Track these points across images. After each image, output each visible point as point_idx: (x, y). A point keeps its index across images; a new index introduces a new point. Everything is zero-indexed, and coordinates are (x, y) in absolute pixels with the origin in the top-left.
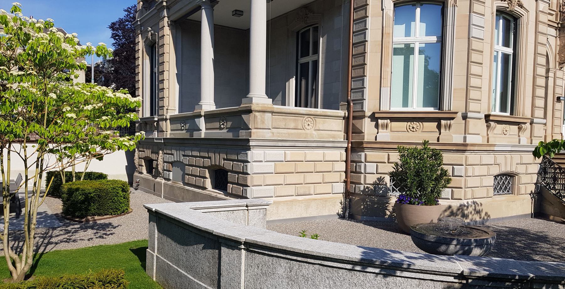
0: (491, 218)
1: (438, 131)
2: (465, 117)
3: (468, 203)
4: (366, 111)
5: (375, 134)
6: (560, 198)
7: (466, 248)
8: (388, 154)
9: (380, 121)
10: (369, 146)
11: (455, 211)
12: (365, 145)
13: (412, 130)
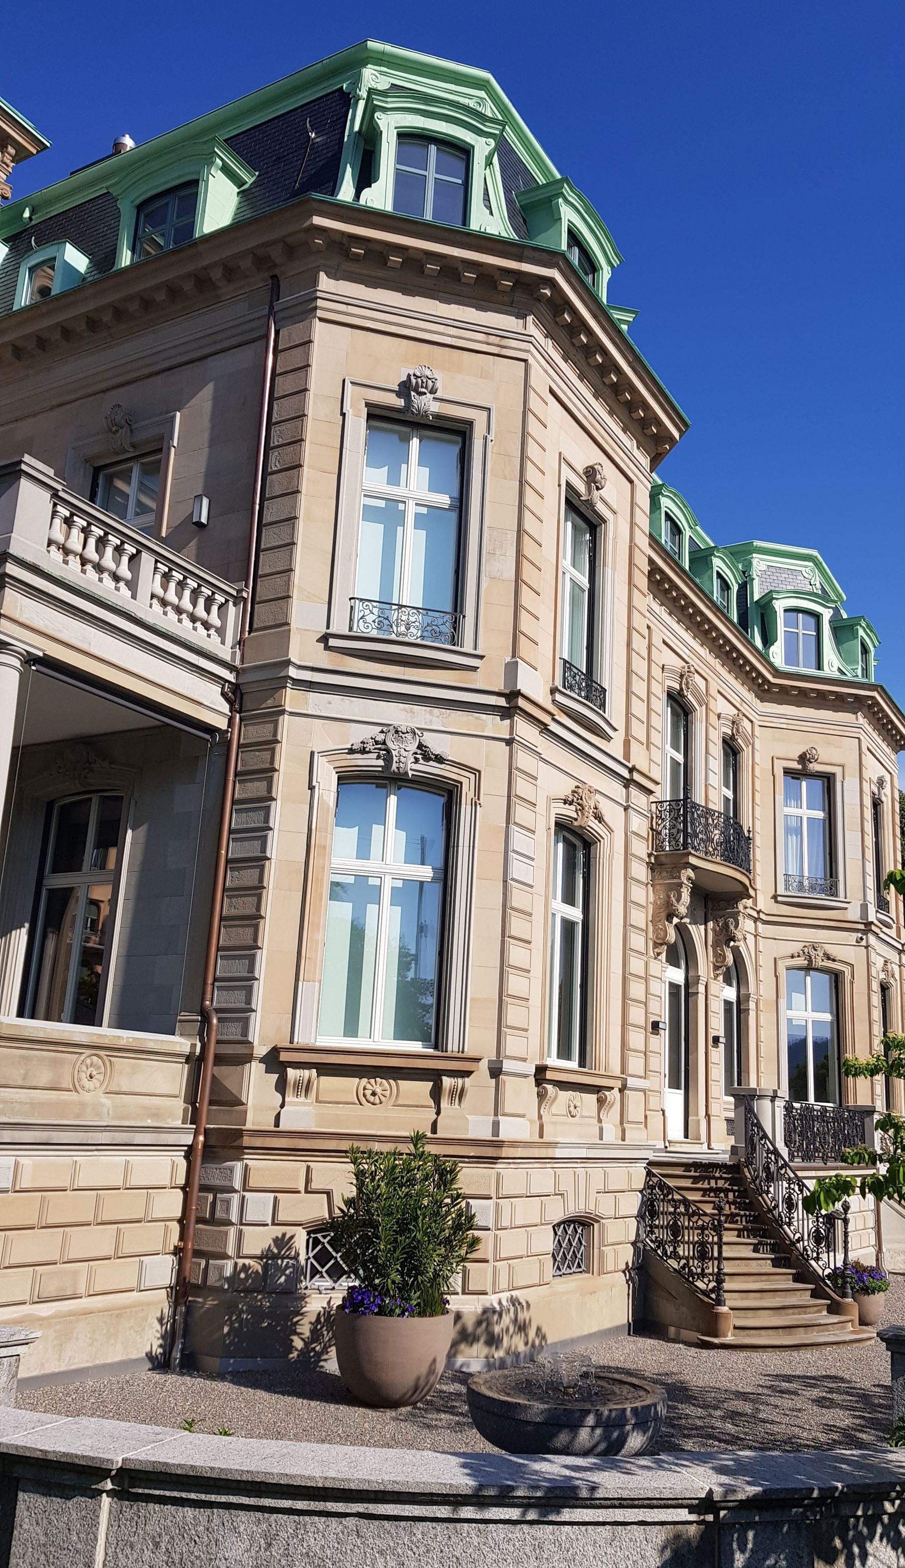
0: (549, 1342)
1: (433, 1105)
2: (496, 1072)
3: (500, 1303)
4: (256, 1043)
5: (275, 1109)
6: (691, 1279)
7: (615, 1434)
8: (308, 1168)
9: (292, 1073)
10: (258, 1142)
11: (470, 1328)
12: (247, 1141)
13: (372, 1099)
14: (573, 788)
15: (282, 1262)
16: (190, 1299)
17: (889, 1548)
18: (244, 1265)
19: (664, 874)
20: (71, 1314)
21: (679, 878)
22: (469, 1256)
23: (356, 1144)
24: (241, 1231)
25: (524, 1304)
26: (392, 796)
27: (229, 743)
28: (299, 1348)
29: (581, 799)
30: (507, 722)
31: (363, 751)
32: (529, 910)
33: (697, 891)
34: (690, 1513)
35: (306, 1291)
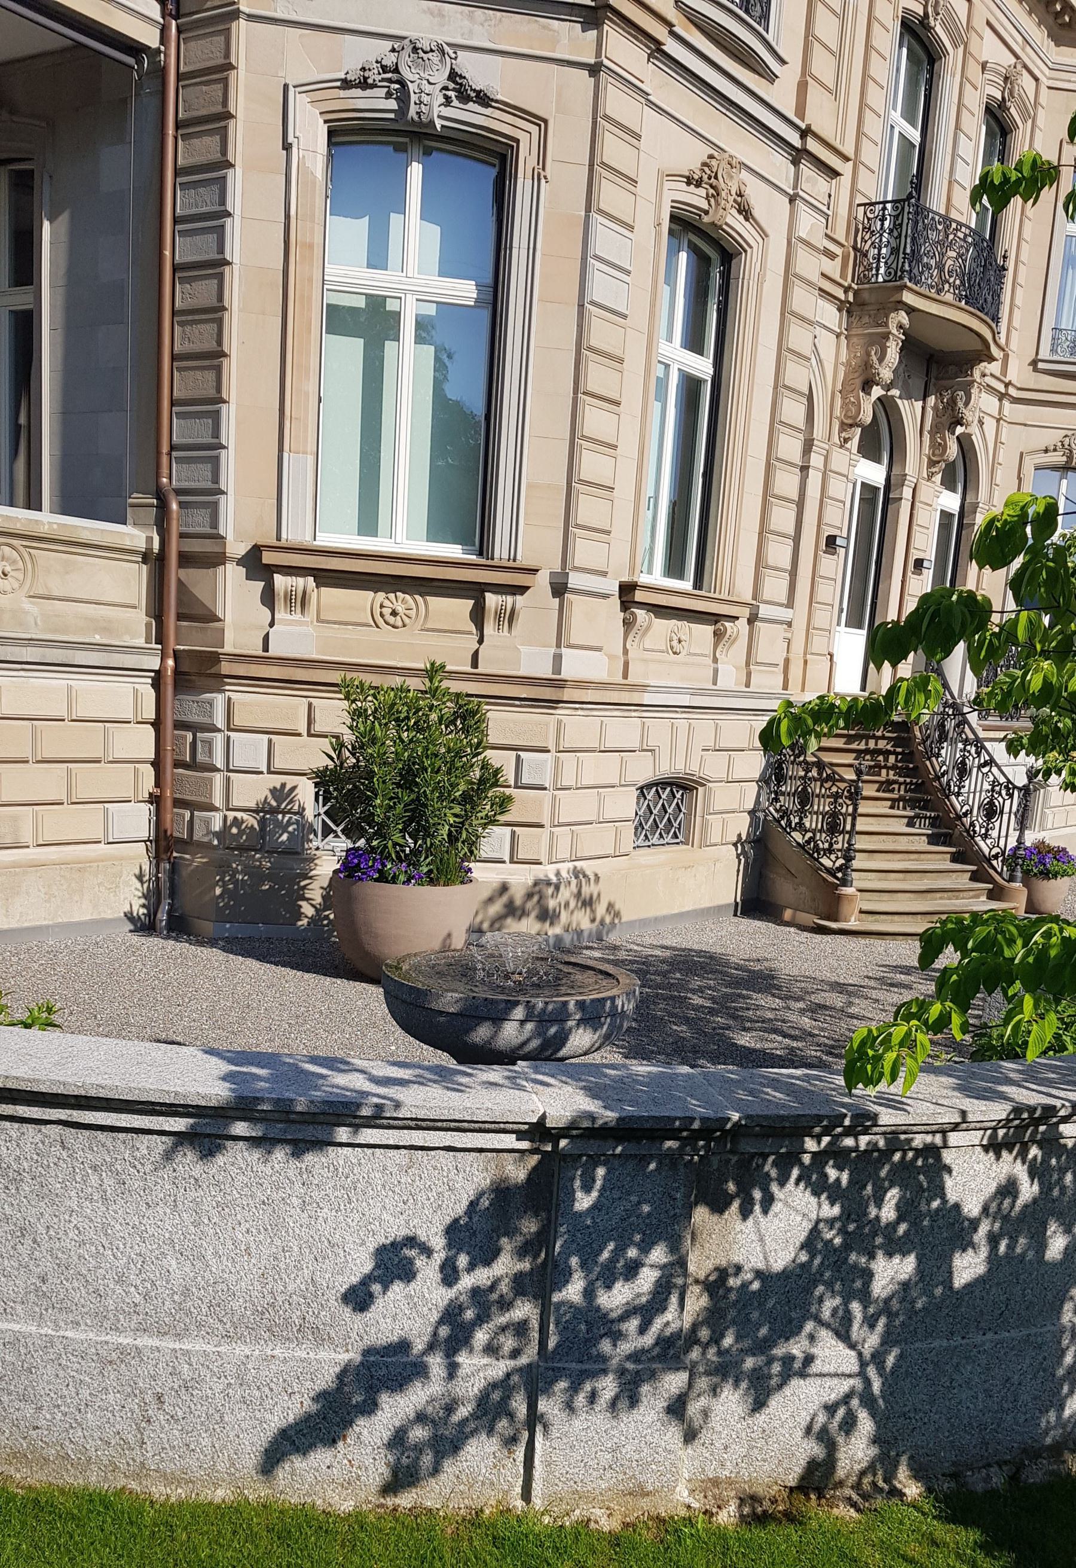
0: (623, 920)
1: (474, 631)
2: (559, 589)
3: (558, 874)
4: (230, 538)
5: (262, 627)
6: (816, 855)
7: (553, 1030)
8: (310, 705)
9: (281, 581)
10: (241, 670)
11: (518, 902)
12: (225, 668)
13: (391, 620)
14: (705, 159)
15: (283, 817)
16: (175, 854)
17: (808, 1193)
18: (235, 818)
19: (866, 319)
20: (15, 865)
21: (886, 325)
22: (498, 817)
23: (349, 676)
24: (228, 779)
25: (592, 878)
26: (414, 164)
27: (163, 71)
28: (310, 915)
29: (716, 178)
30: (593, 34)
31: (364, 84)
32: (618, 353)
33: (911, 346)
34: (518, 1140)
35: (317, 852)
